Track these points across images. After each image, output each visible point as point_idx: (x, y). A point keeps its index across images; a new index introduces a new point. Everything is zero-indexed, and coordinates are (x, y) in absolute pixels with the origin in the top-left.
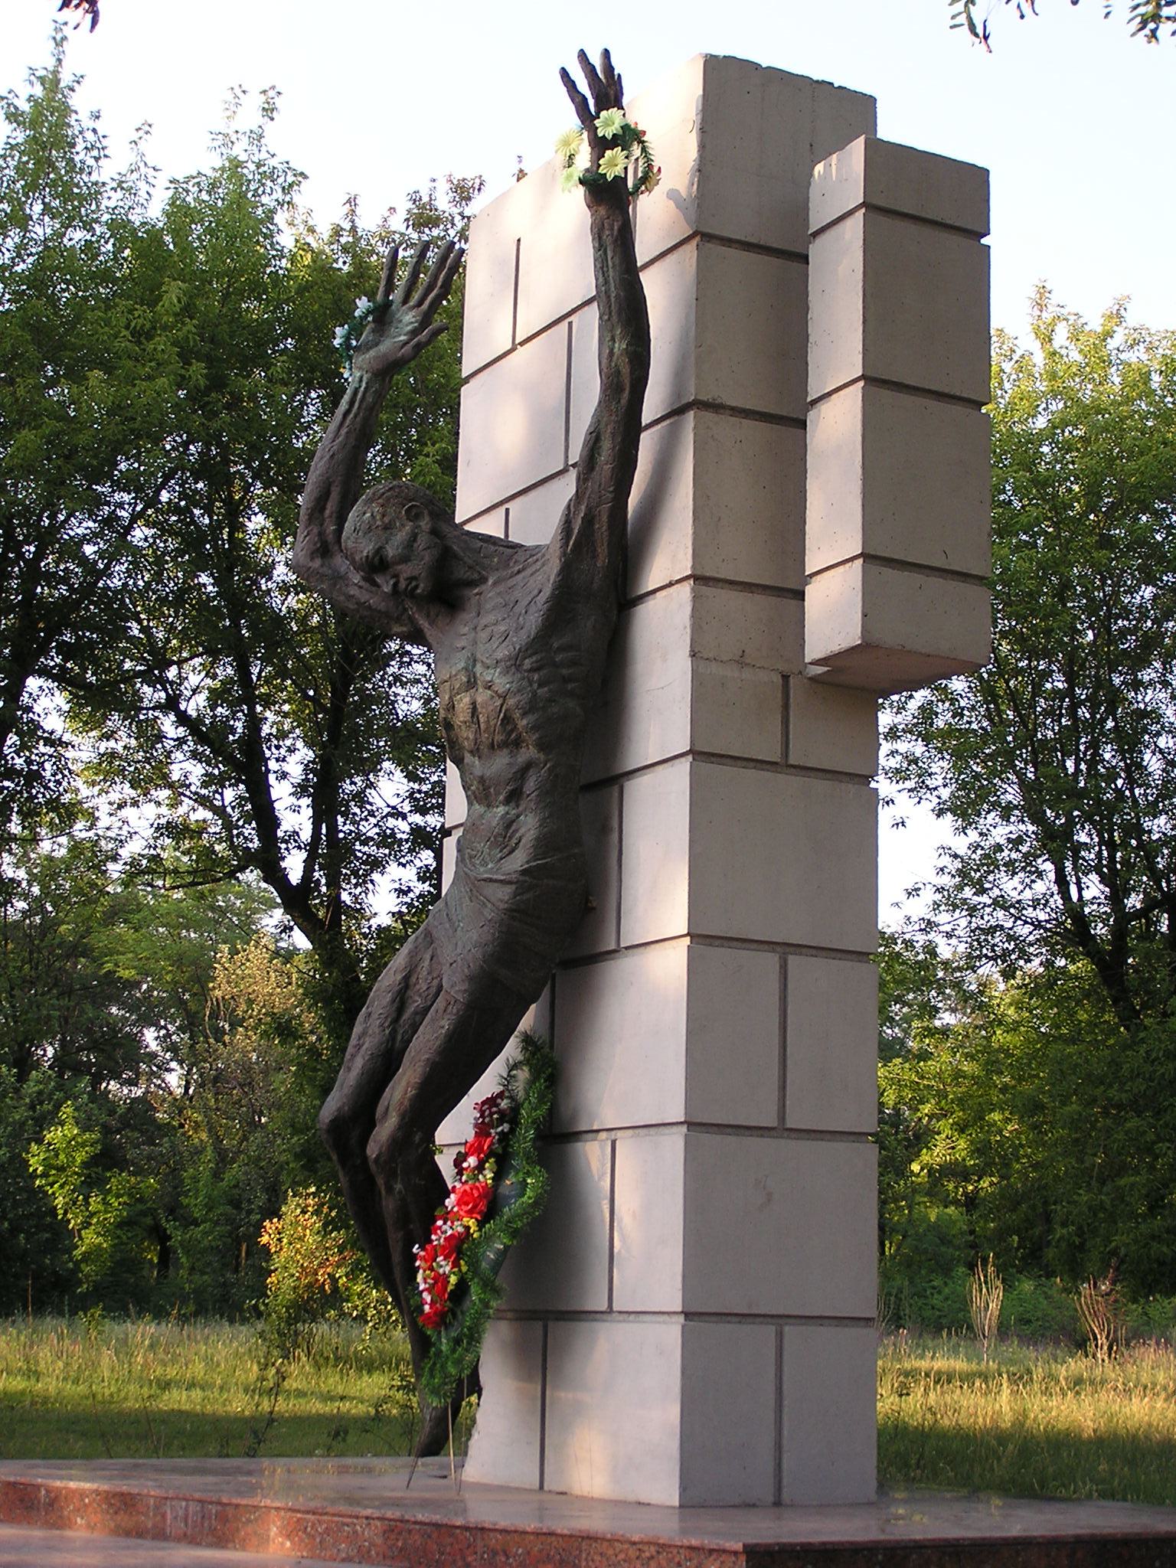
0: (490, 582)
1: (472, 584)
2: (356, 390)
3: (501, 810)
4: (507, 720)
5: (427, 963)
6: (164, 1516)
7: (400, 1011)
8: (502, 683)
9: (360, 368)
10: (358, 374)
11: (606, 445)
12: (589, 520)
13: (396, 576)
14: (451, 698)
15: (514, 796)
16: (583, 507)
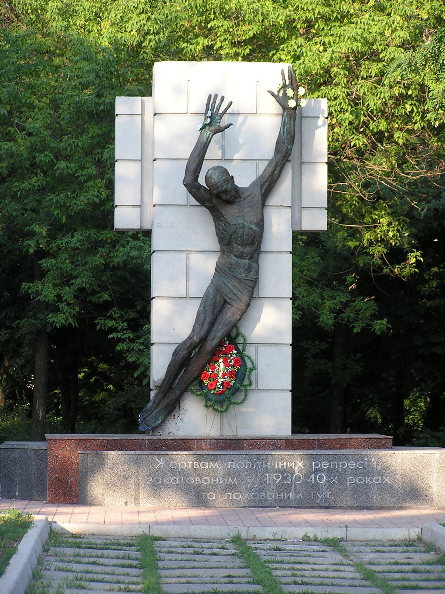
0: (242, 199)
1: (236, 198)
2: (208, 137)
3: (247, 261)
4: (253, 239)
5: (218, 299)
6: (201, 444)
7: (214, 311)
8: (256, 229)
9: (211, 131)
10: (209, 133)
11: (278, 169)
12: (267, 187)
13: (227, 195)
14: (236, 230)
15: (250, 259)
16: (267, 184)
